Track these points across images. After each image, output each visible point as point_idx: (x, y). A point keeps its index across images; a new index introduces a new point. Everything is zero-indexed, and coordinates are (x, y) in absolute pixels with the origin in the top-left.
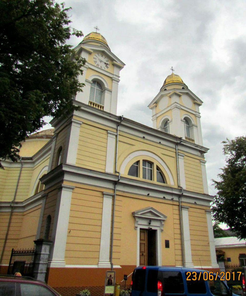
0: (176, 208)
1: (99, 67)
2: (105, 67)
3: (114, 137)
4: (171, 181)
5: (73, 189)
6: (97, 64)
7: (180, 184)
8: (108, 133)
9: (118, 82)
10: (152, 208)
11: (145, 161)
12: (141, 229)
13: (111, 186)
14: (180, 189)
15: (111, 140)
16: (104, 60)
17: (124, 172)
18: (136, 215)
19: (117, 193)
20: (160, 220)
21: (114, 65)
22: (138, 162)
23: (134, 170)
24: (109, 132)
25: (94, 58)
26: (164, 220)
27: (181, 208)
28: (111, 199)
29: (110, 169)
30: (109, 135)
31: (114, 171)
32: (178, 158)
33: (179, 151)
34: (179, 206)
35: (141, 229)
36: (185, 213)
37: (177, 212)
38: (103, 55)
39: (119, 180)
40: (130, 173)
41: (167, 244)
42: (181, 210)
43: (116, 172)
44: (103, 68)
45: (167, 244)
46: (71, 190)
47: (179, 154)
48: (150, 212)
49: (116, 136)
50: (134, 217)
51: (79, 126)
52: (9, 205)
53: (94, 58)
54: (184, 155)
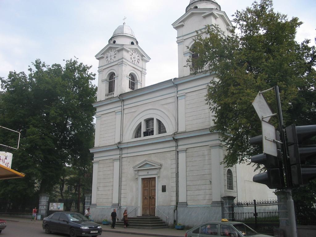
0: (174, 153)
2: (114, 59)
4: (170, 130)
5: (98, 162)
8: (116, 113)
10: (146, 161)
12: (143, 179)
19: (123, 156)
21: (119, 51)
23: (138, 133)
28: (119, 162)
35: (143, 179)
36: (182, 156)
37: (174, 157)
41: (164, 189)
45: (164, 189)
46: (98, 163)
48: (147, 164)
52: (120, 177)
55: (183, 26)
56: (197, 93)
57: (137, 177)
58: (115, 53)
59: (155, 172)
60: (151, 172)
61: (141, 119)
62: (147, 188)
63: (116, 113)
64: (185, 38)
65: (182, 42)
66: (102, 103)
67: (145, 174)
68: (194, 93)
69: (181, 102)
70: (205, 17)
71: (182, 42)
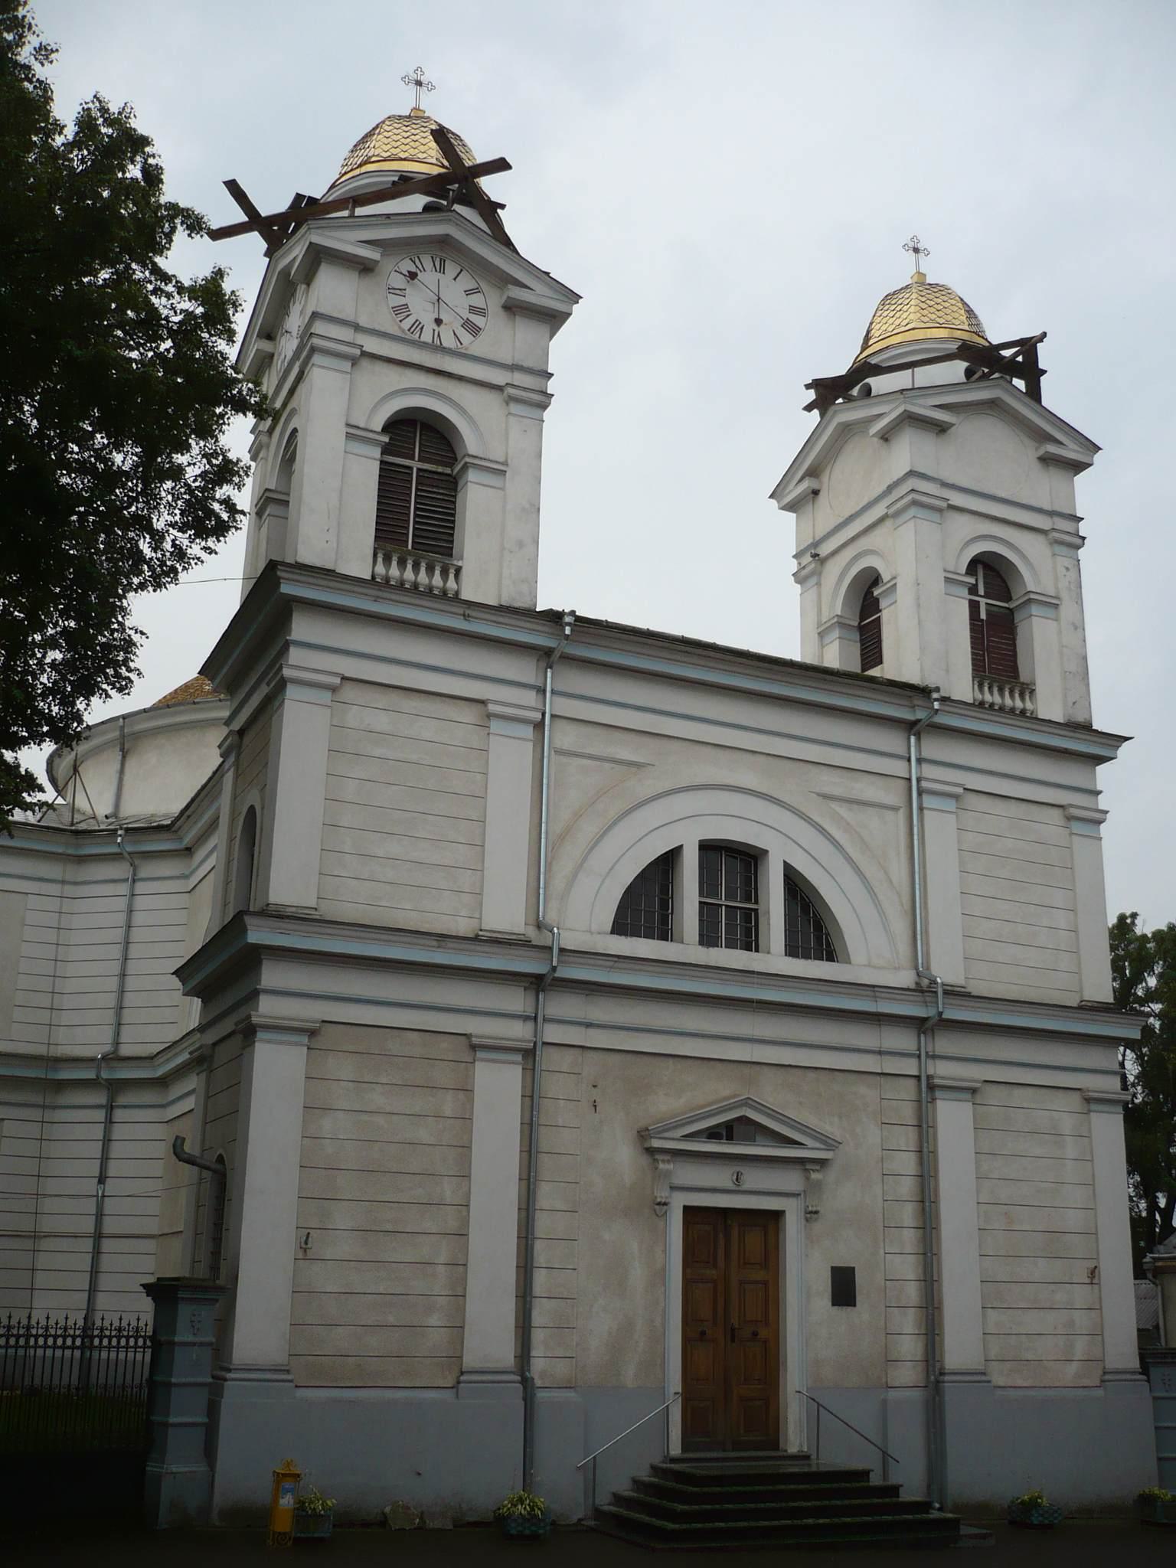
0: (907, 1091)
1: (427, 337)
3: (528, 731)
4: (873, 952)
6: (410, 321)
7: (927, 955)
9: (544, 406)
10: (747, 1103)
11: (709, 849)
12: (688, 1210)
13: (516, 1000)
14: (925, 989)
15: (510, 756)
16: (454, 289)
17: (586, 916)
18: (656, 1143)
19: (552, 1033)
20: (801, 1161)
21: (512, 308)
22: (669, 861)
23: (647, 904)
24: (492, 707)
25: (392, 290)
26: (822, 1163)
27: (930, 1089)
28: (518, 1071)
29: (505, 913)
30: (495, 726)
31: (532, 920)
32: (921, 809)
33: (929, 771)
34: (918, 1078)
35: (685, 1207)
38: (443, 261)
39: (554, 969)
40: (620, 927)
42: (934, 1099)
43: (539, 926)
44: (448, 341)
47: (924, 784)
49: (539, 726)
50: (651, 1151)
51: (326, 696)
53: (392, 290)
54: (961, 790)
55: (941, 429)
56: (1014, 809)
57: (662, 1194)
58: (477, 300)
59: (791, 1180)
60: (755, 1178)
61: (686, 826)
62: (711, 1273)
63: (489, 716)
64: (958, 499)
65: (940, 510)
66: (376, 599)
67: (712, 1186)
68: (999, 807)
69: (940, 827)
70: (1047, 460)
71: (940, 510)
